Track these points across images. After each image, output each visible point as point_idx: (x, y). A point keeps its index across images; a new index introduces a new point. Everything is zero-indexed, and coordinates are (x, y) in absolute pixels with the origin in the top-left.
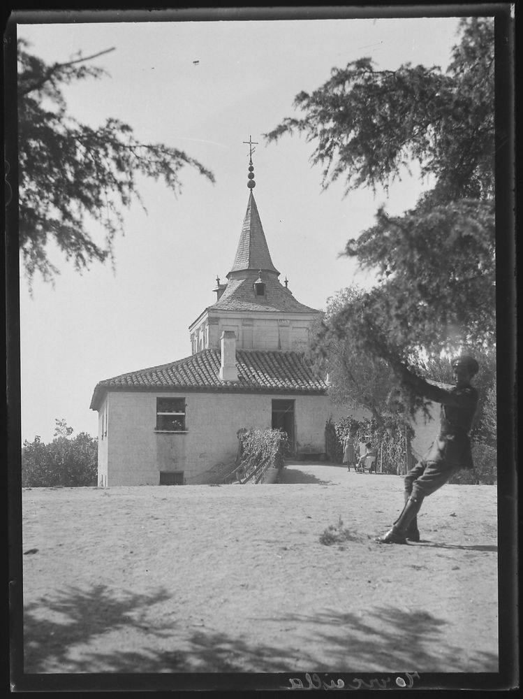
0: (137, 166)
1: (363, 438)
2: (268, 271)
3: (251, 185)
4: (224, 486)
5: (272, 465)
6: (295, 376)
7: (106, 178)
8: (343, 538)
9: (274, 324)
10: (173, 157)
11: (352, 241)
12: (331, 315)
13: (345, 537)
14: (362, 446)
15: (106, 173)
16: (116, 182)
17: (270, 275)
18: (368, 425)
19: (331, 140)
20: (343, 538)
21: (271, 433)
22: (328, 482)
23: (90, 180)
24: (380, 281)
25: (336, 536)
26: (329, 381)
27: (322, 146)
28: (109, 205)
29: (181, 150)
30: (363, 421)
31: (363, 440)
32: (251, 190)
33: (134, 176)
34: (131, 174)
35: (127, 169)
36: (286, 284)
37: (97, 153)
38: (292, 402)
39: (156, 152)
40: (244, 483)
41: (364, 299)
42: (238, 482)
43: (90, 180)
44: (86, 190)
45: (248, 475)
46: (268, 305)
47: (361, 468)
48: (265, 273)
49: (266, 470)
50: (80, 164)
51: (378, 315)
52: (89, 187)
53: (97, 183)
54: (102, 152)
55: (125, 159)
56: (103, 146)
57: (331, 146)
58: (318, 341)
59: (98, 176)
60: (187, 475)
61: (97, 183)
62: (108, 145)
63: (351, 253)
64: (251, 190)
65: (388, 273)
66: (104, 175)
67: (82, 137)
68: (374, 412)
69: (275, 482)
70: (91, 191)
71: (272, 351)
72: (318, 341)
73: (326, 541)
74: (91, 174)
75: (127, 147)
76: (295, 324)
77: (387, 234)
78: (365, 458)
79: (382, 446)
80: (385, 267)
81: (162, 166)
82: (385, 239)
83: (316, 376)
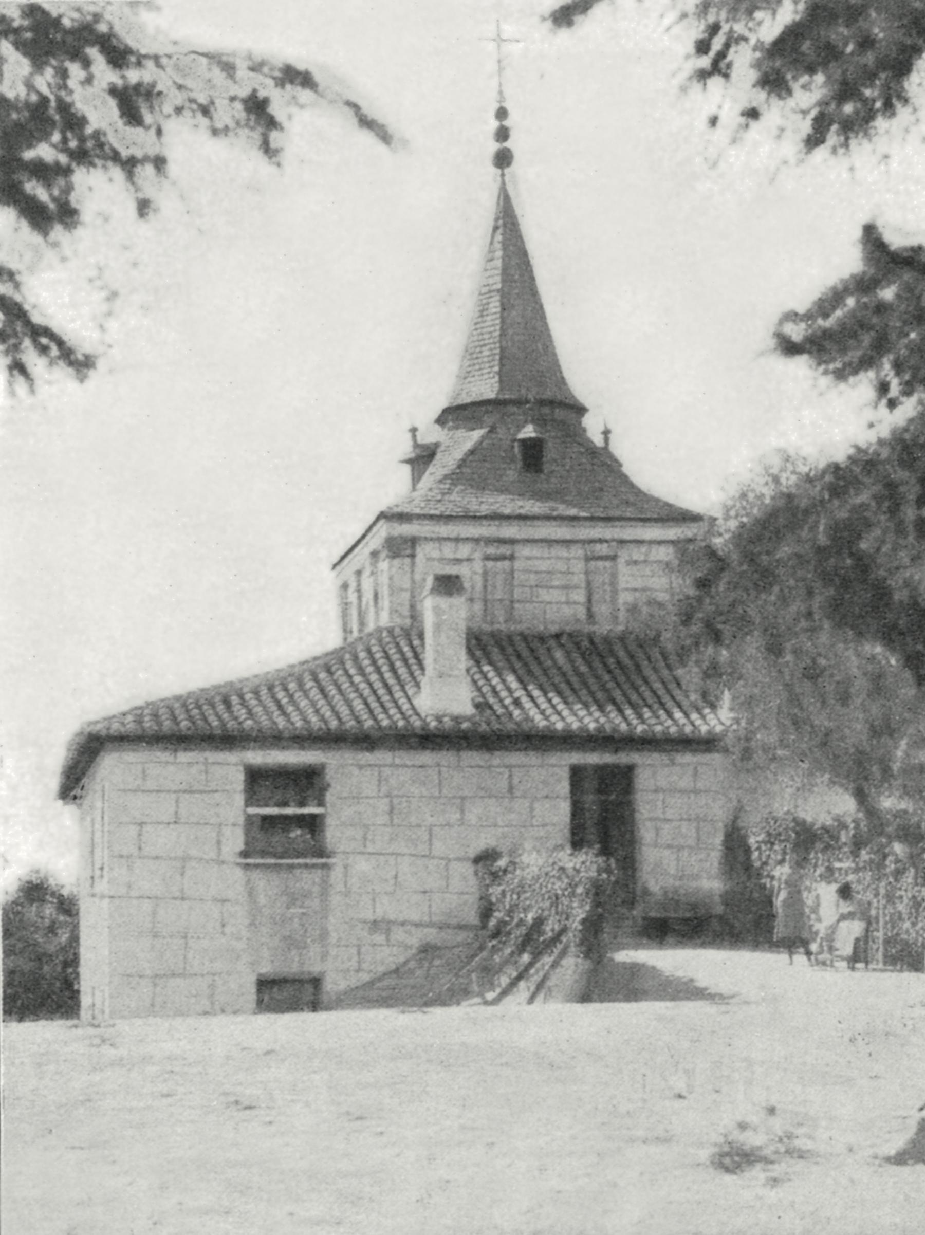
0: (179, 110)
1: (830, 870)
2: (551, 403)
3: (503, 159)
4: (438, 1012)
5: (573, 949)
6: (634, 697)
7: (90, 144)
8: (777, 1152)
9: (577, 551)
10: (281, 83)
11: (792, 316)
12: (733, 524)
13: (783, 1150)
14: (827, 893)
15: (89, 130)
16: (115, 157)
17: (559, 414)
18: (843, 833)
19: (725, 28)
20: (777, 1152)
21: (569, 860)
22: (732, 997)
23: (44, 152)
24: (871, 425)
25: (760, 1148)
26: (731, 709)
27: (702, 47)
28: (99, 221)
29: (301, 66)
30: (829, 822)
31: (829, 874)
32: (503, 175)
33: (165, 139)
34: (159, 132)
35: (148, 118)
36: (607, 440)
37: (63, 74)
38: (629, 770)
39: (229, 68)
40: (496, 1001)
41: (828, 478)
42: (477, 1000)
43: (44, 152)
44: (34, 182)
45: (504, 980)
46: (555, 500)
47: (825, 956)
48: (546, 410)
49: (555, 965)
50: (17, 110)
51: (868, 525)
52: (42, 171)
53: (63, 159)
54: (75, 70)
55: (142, 90)
56: (77, 55)
57: (727, 46)
58: (699, 600)
59: (65, 140)
60: (333, 984)
61: (63, 159)
62: (93, 52)
63: (790, 348)
64: (503, 175)
65: (892, 404)
66: (82, 139)
67: (16, 31)
68: (861, 795)
69: (585, 998)
70: (48, 186)
71: (568, 629)
72: (699, 600)
73: (727, 1161)
74: (45, 136)
75: (146, 56)
76: (638, 554)
77: (888, 294)
78: (833, 929)
79: (882, 891)
80: (883, 388)
81: (248, 110)
82: (881, 308)
83: (693, 697)
